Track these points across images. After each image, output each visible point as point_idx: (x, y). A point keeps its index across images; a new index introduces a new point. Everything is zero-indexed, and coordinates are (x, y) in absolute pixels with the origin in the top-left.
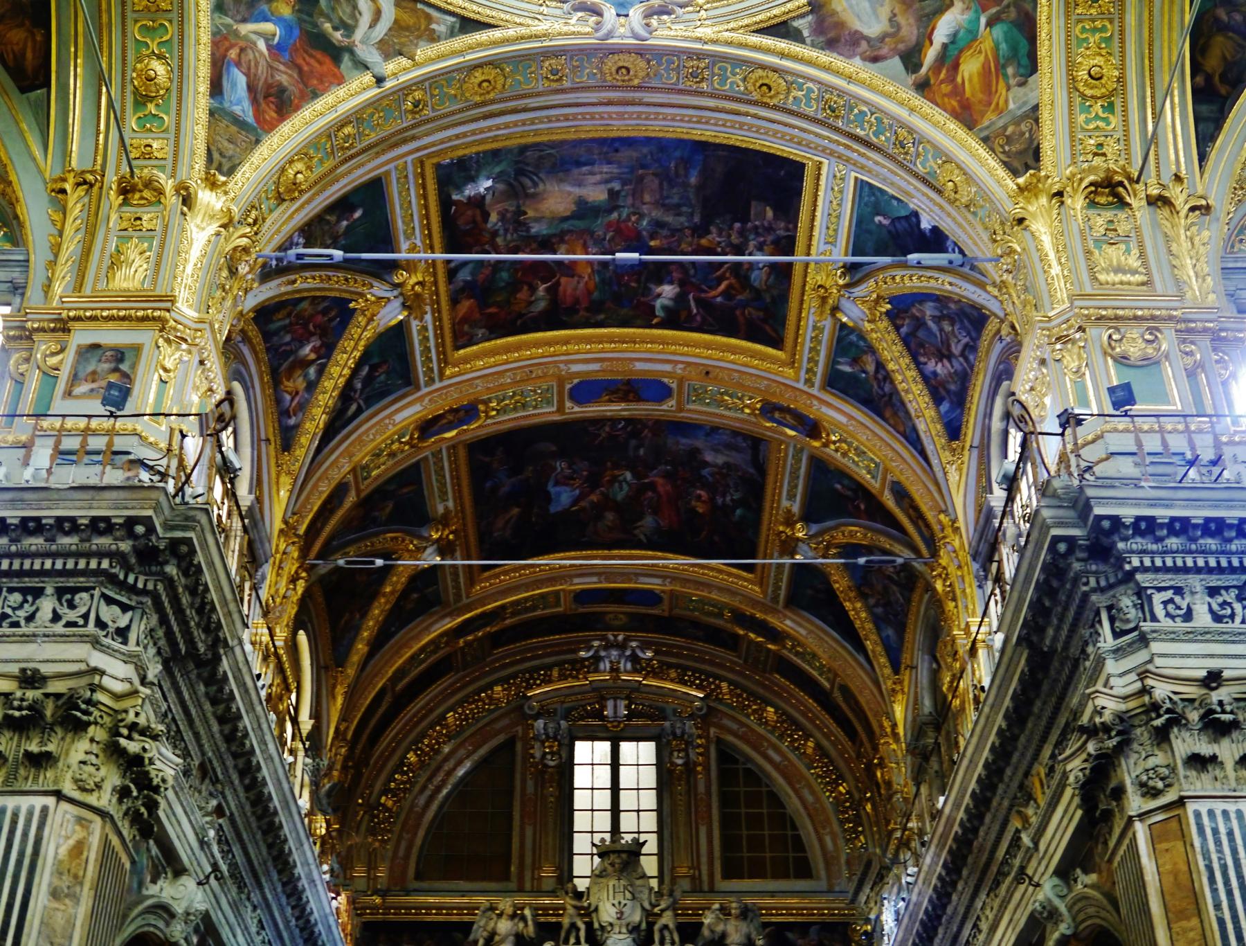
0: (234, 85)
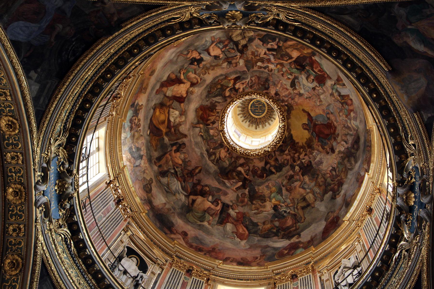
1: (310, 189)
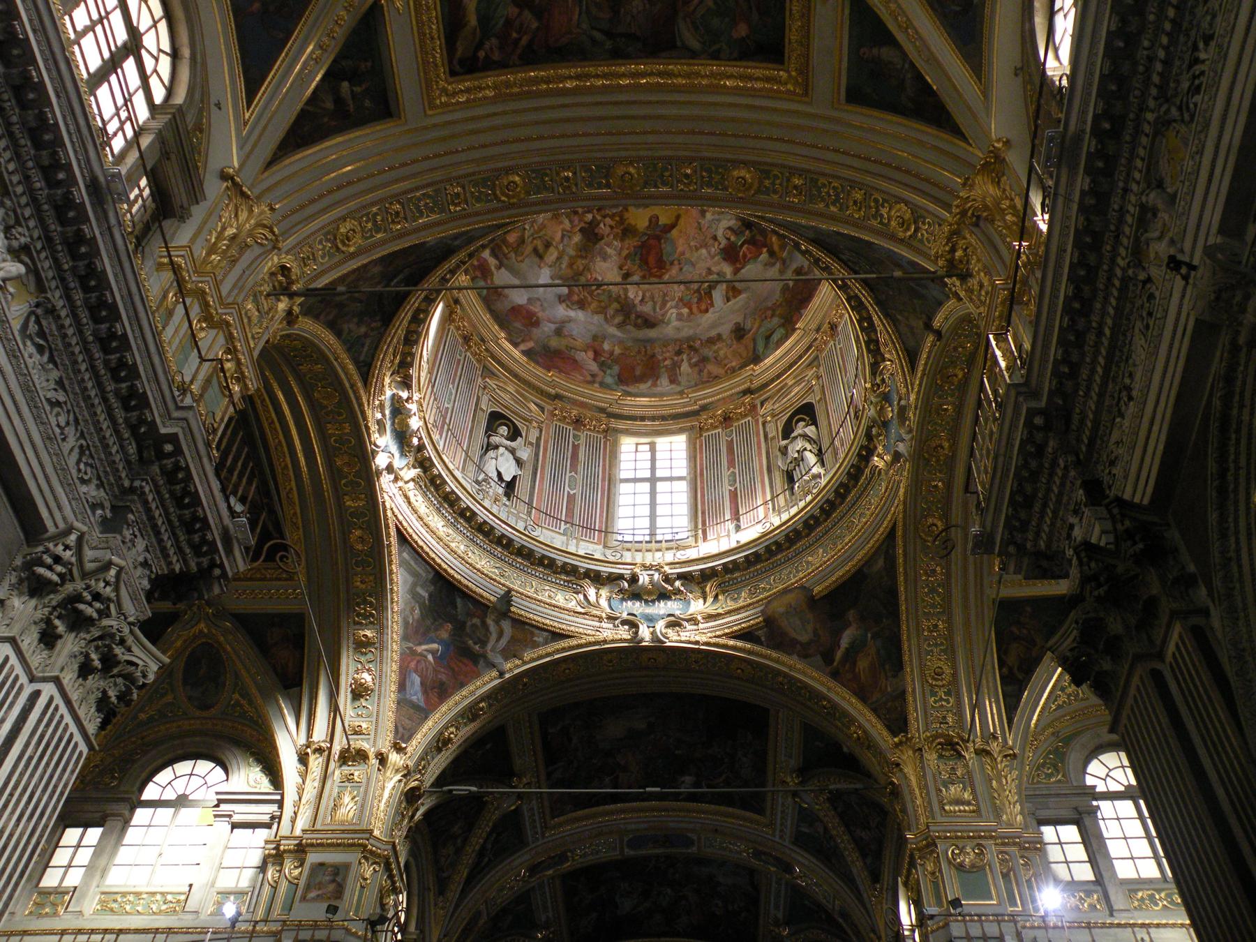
0: (413, 683)
1: (564, 250)
